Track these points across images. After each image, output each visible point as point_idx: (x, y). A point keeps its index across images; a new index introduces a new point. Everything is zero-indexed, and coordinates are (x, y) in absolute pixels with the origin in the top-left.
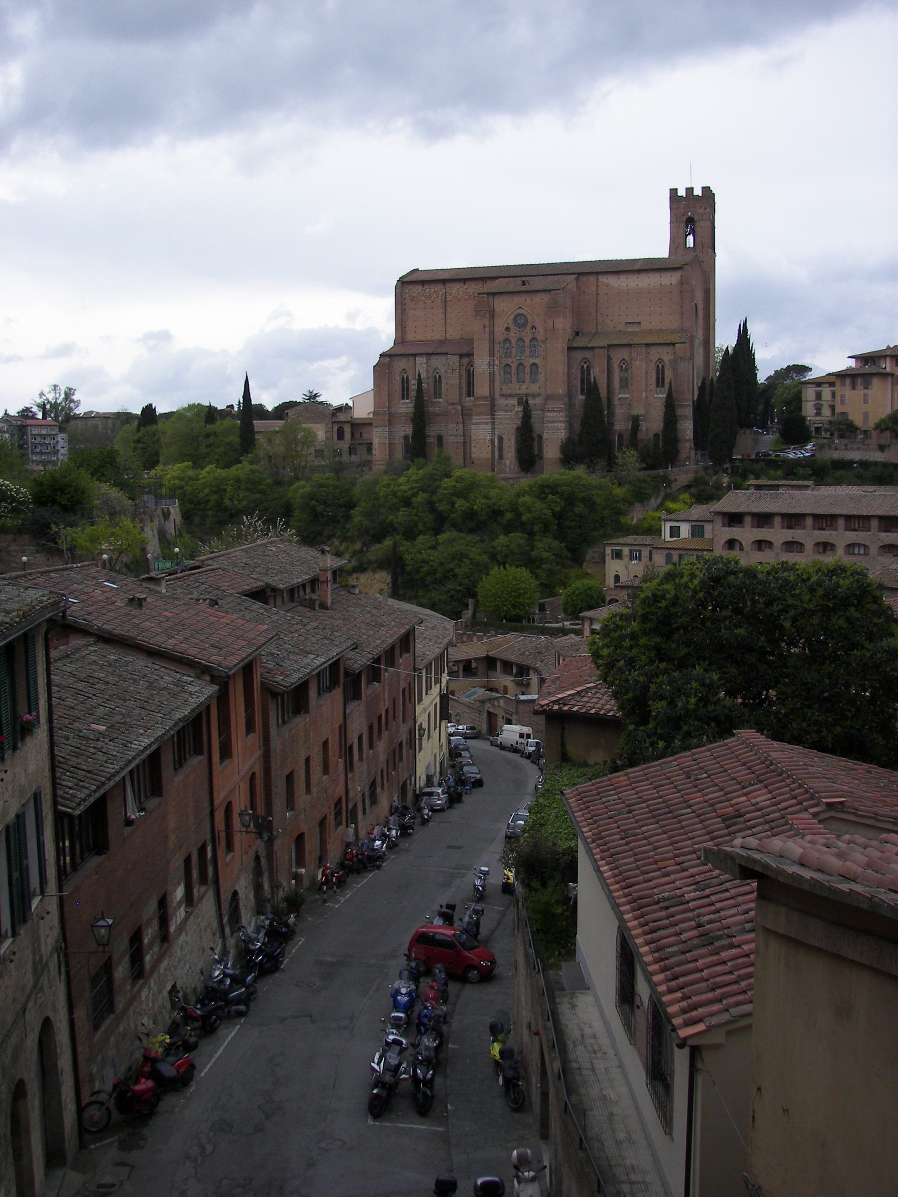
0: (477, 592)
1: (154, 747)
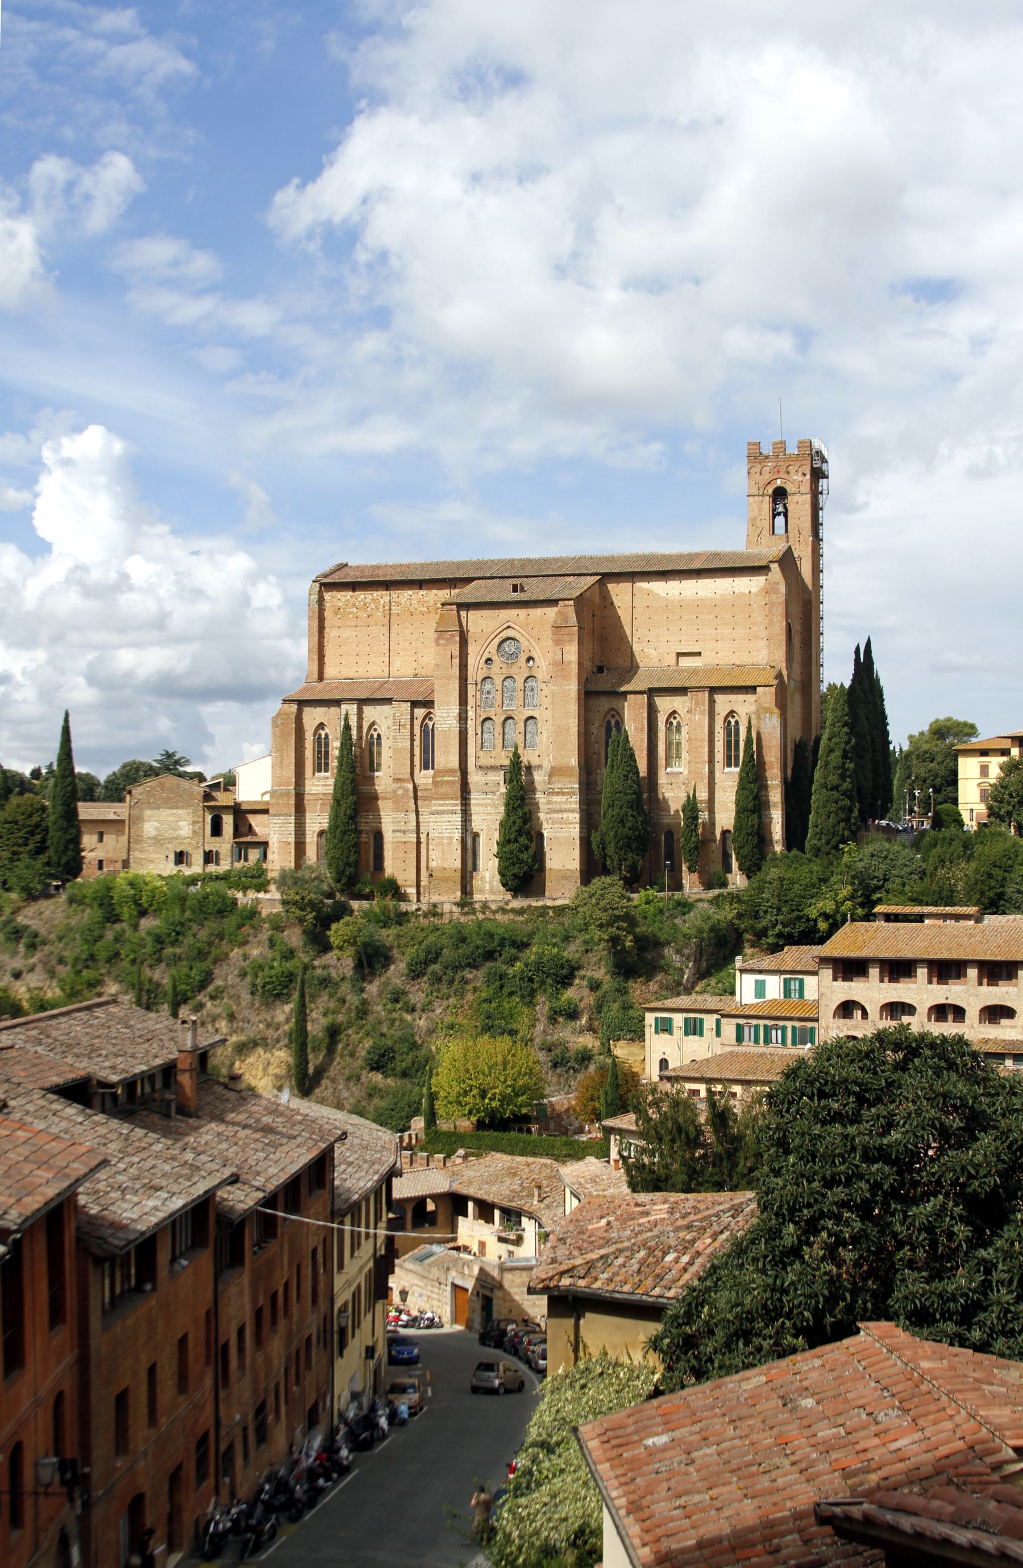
0: (267, 870)
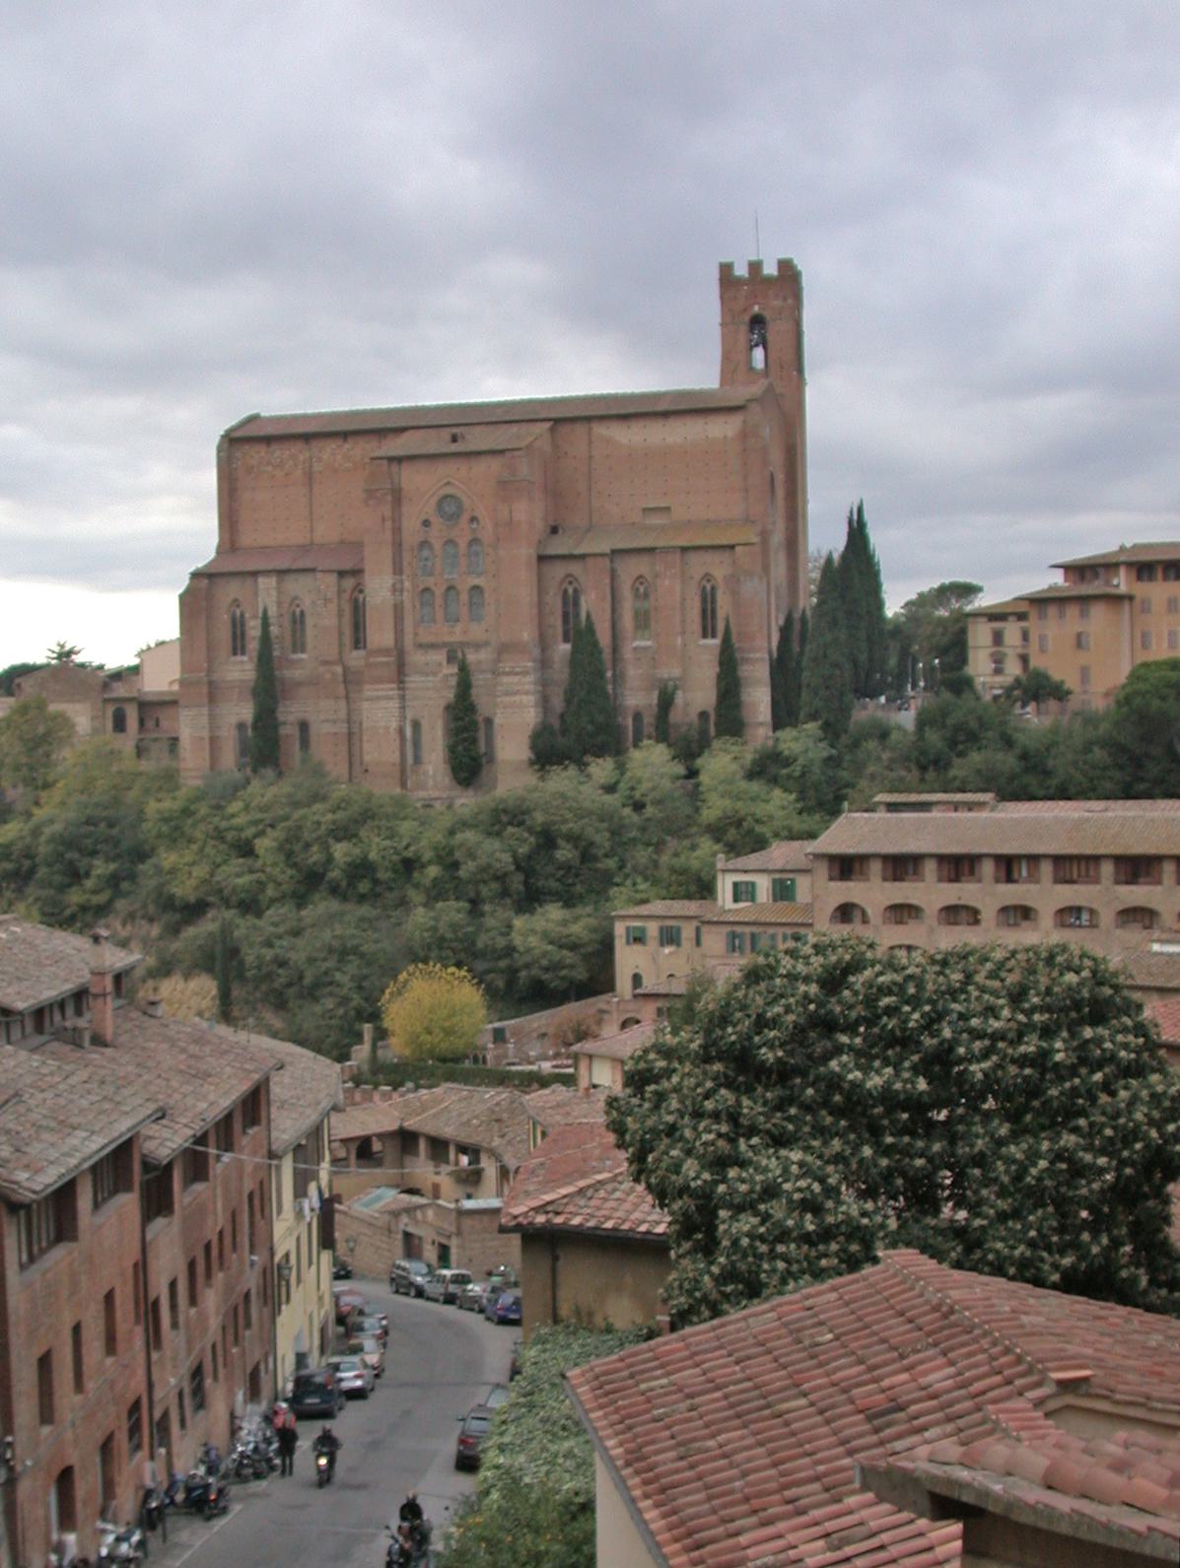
1: (128, 1135)
